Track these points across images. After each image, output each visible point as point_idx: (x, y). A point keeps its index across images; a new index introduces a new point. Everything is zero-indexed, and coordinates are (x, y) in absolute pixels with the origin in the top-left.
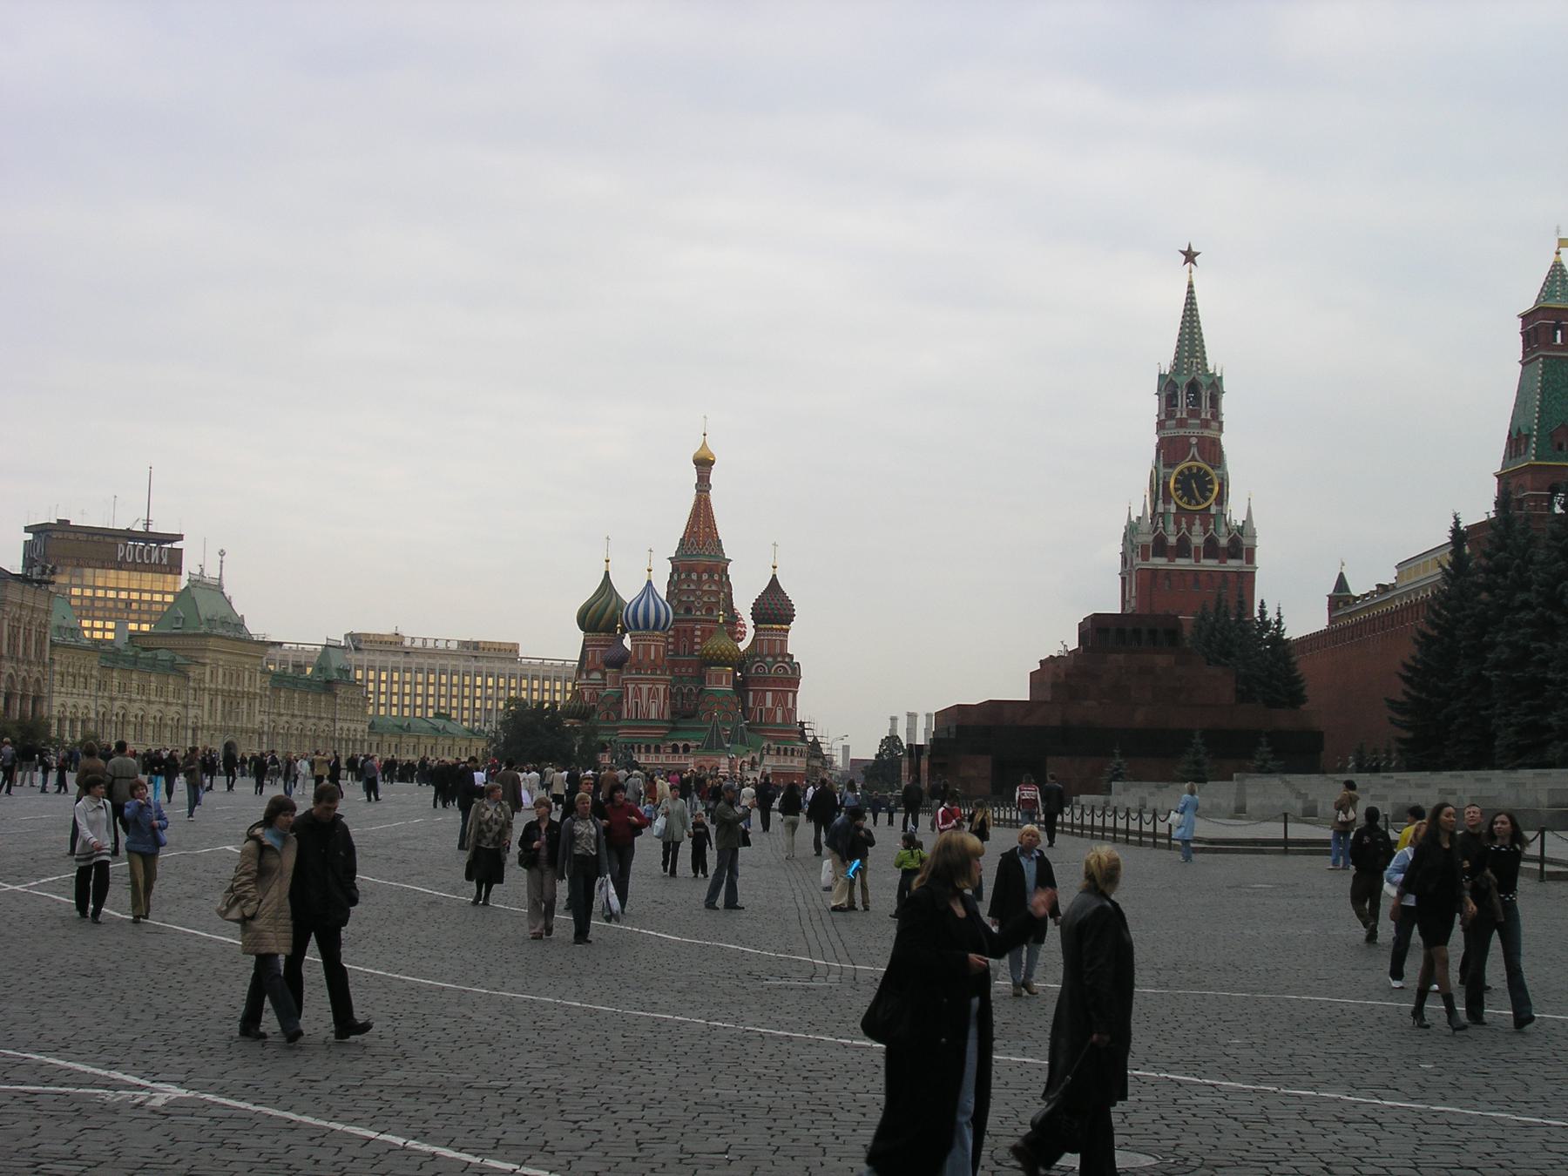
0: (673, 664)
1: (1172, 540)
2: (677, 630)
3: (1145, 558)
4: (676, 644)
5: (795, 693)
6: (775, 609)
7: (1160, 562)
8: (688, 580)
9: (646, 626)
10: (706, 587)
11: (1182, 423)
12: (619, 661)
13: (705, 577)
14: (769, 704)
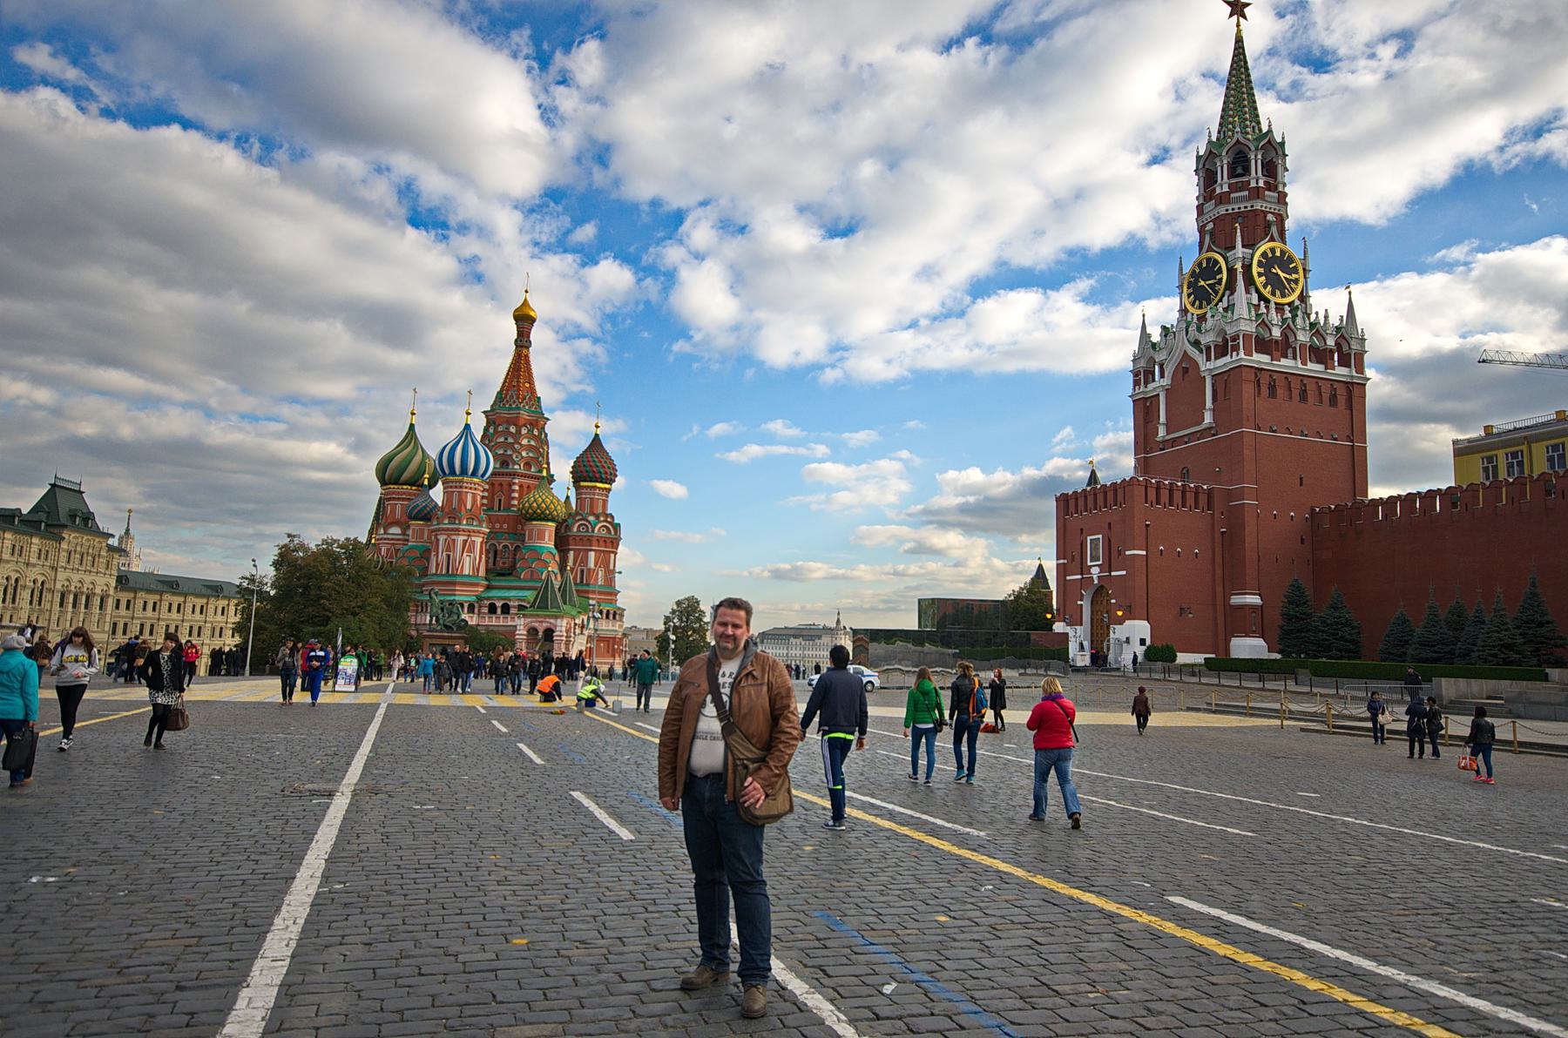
0: (490, 520)
1: (1277, 333)
4: (491, 499)
6: (594, 467)
7: (1261, 359)
8: (507, 433)
9: (464, 471)
10: (525, 442)
11: (1257, 193)
13: (524, 431)
14: (592, 565)
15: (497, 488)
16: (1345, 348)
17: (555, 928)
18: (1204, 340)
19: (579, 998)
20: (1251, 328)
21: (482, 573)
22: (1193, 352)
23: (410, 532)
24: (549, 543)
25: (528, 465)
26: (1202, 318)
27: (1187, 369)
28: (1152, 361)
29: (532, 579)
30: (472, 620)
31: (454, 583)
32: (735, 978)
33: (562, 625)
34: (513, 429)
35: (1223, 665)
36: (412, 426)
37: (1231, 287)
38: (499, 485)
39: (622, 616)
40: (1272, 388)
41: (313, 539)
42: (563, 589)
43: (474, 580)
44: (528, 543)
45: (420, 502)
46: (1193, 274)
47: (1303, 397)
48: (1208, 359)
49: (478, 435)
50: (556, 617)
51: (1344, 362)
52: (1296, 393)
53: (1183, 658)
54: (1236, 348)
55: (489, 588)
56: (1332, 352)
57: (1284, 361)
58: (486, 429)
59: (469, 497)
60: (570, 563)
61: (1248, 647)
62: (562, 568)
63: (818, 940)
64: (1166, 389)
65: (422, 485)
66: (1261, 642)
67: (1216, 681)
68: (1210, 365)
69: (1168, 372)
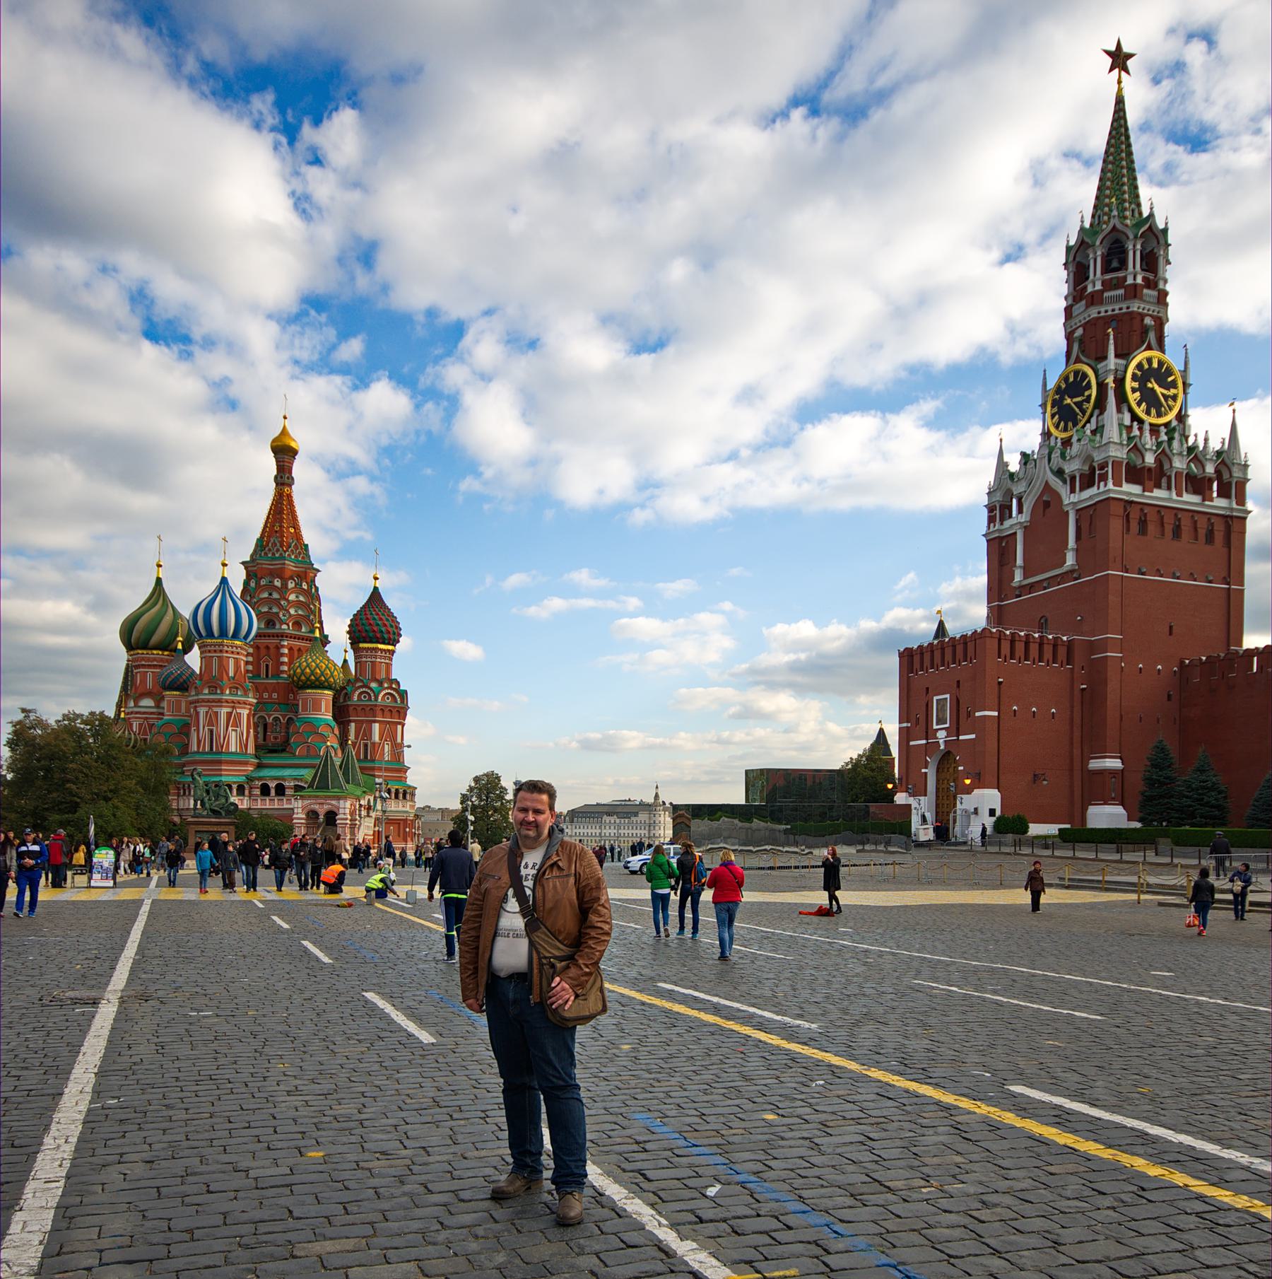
0: (258, 689)
2: (257, 648)
3: (1118, 483)
4: (256, 664)
5: (403, 725)
7: (1131, 490)
10: (292, 597)
12: (182, 684)
14: (376, 738)
15: (263, 651)
16: (1226, 476)
17: (353, 1139)
19: (383, 1212)
20: (1120, 453)
21: (251, 749)
22: (1056, 483)
23: (165, 704)
24: (326, 715)
25: (297, 625)
26: (1067, 443)
27: (1048, 504)
28: (1009, 495)
29: (307, 757)
30: (243, 803)
31: (220, 762)
32: (548, 1185)
33: (345, 807)
34: (278, 583)
35: (1078, 836)
38: (265, 648)
39: (413, 795)
40: (1143, 523)
41: (52, 713)
42: (345, 766)
43: (242, 758)
45: (174, 669)
47: (1177, 533)
48: (1073, 491)
49: (237, 589)
50: (338, 798)
51: (1224, 493)
52: (1169, 529)
53: (1035, 829)
54: (1104, 478)
55: (260, 766)
56: (1210, 481)
57: (1157, 493)
58: (246, 584)
59: (231, 662)
60: (352, 737)
61: (1106, 815)
62: (343, 741)
63: (637, 1143)
64: (1023, 523)
65: (175, 650)
66: (1120, 810)
67: (1070, 854)
68: (1074, 498)
69: (1027, 507)
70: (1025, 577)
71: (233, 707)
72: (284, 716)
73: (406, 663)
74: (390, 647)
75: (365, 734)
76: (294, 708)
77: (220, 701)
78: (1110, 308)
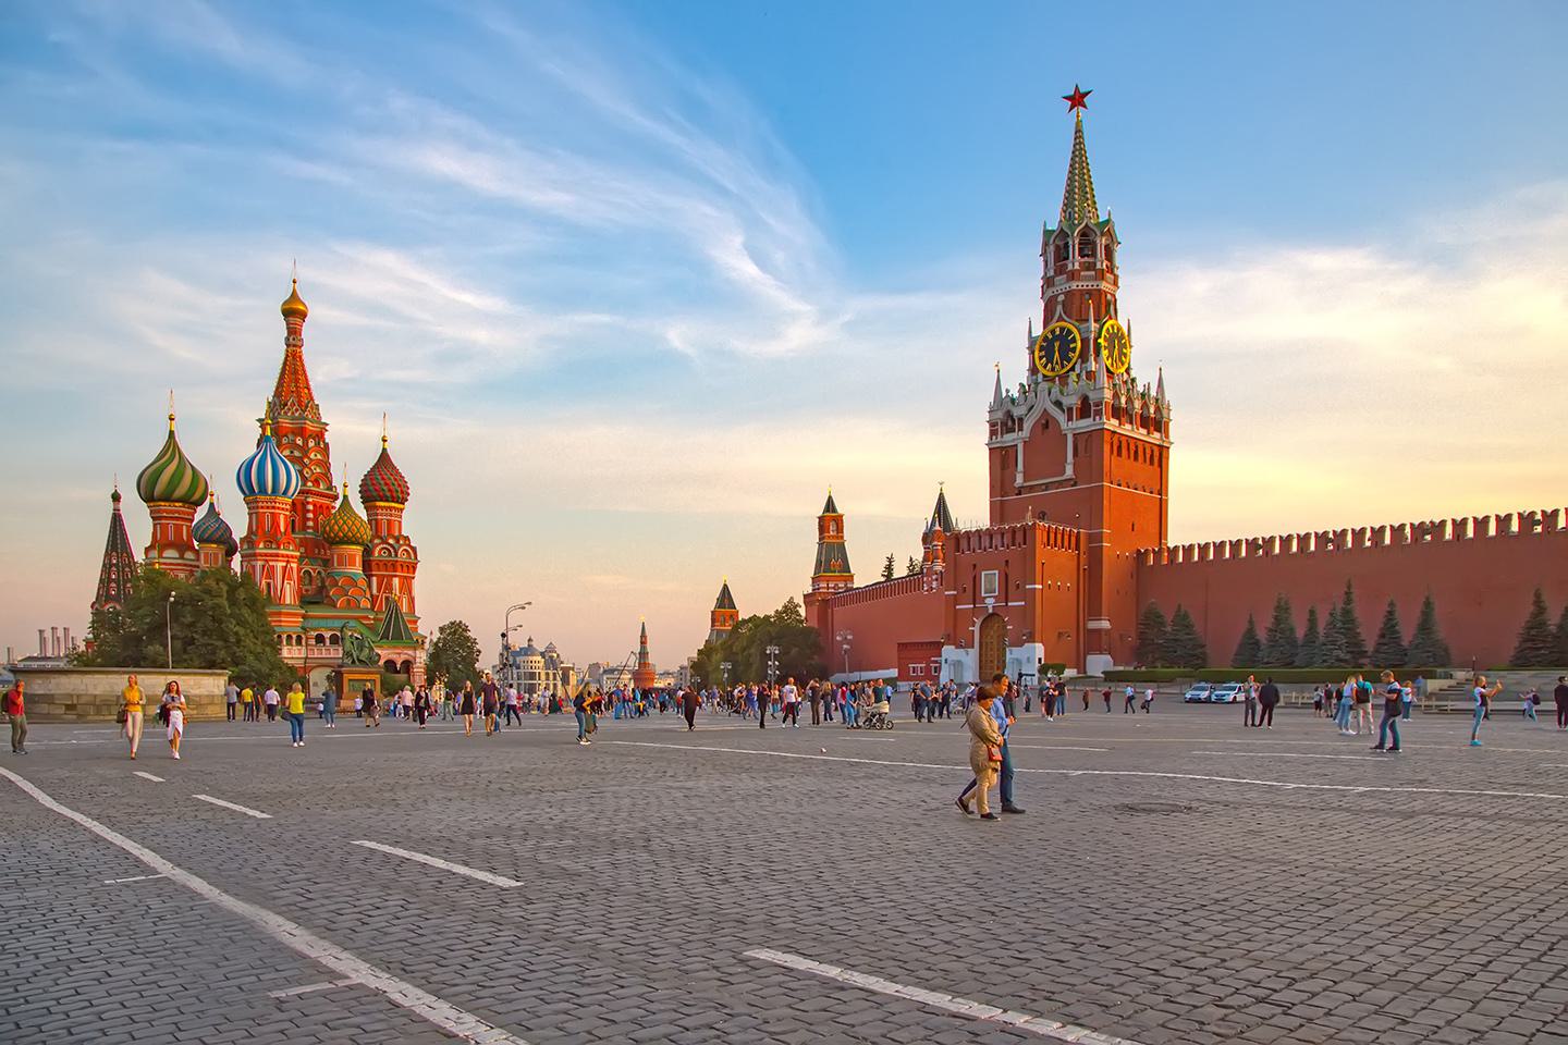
6: (384, 485)
13: (311, 444)
18: (1066, 402)
36: (171, 433)
37: (1084, 357)
44: (337, 568)
46: (1045, 339)
48: (1070, 419)
57: (1128, 426)
69: (1027, 425)
70: (1025, 481)
71: (288, 562)
72: (314, 570)
73: (412, 521)
74: (401, 506)
75: (386, 588)
76: (327, 563)
77: (277, 555)
78: (1080, 284)
